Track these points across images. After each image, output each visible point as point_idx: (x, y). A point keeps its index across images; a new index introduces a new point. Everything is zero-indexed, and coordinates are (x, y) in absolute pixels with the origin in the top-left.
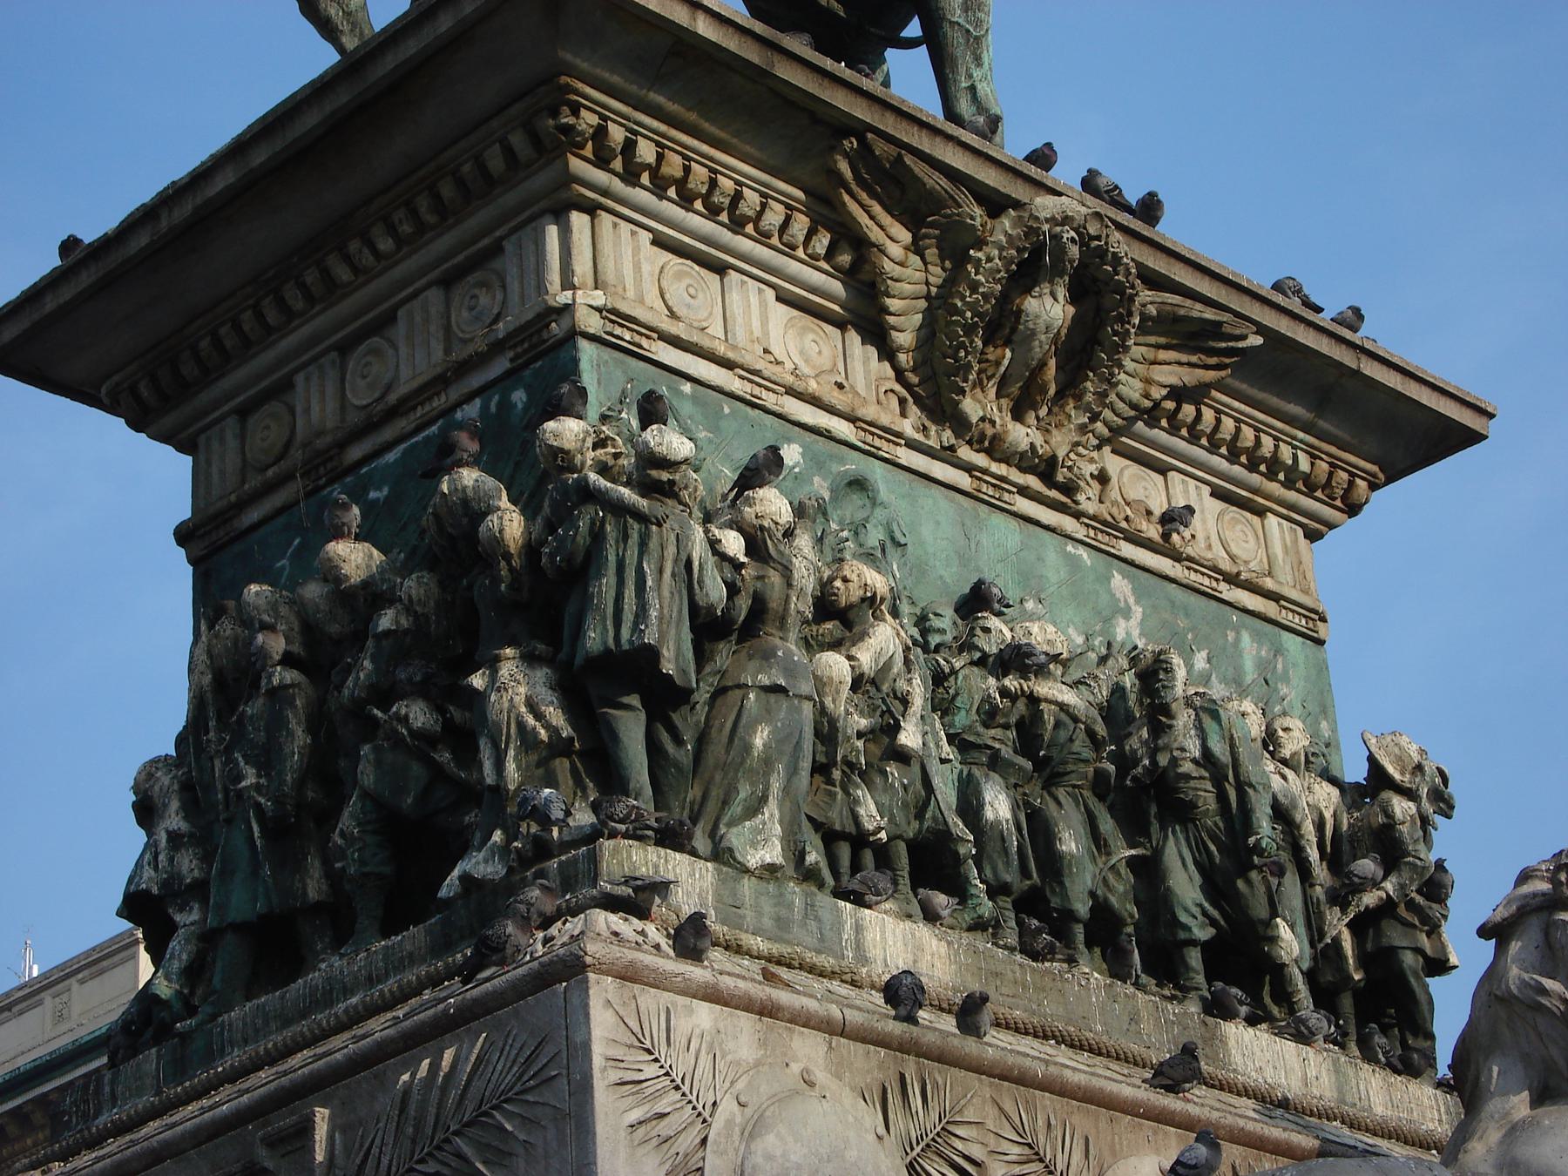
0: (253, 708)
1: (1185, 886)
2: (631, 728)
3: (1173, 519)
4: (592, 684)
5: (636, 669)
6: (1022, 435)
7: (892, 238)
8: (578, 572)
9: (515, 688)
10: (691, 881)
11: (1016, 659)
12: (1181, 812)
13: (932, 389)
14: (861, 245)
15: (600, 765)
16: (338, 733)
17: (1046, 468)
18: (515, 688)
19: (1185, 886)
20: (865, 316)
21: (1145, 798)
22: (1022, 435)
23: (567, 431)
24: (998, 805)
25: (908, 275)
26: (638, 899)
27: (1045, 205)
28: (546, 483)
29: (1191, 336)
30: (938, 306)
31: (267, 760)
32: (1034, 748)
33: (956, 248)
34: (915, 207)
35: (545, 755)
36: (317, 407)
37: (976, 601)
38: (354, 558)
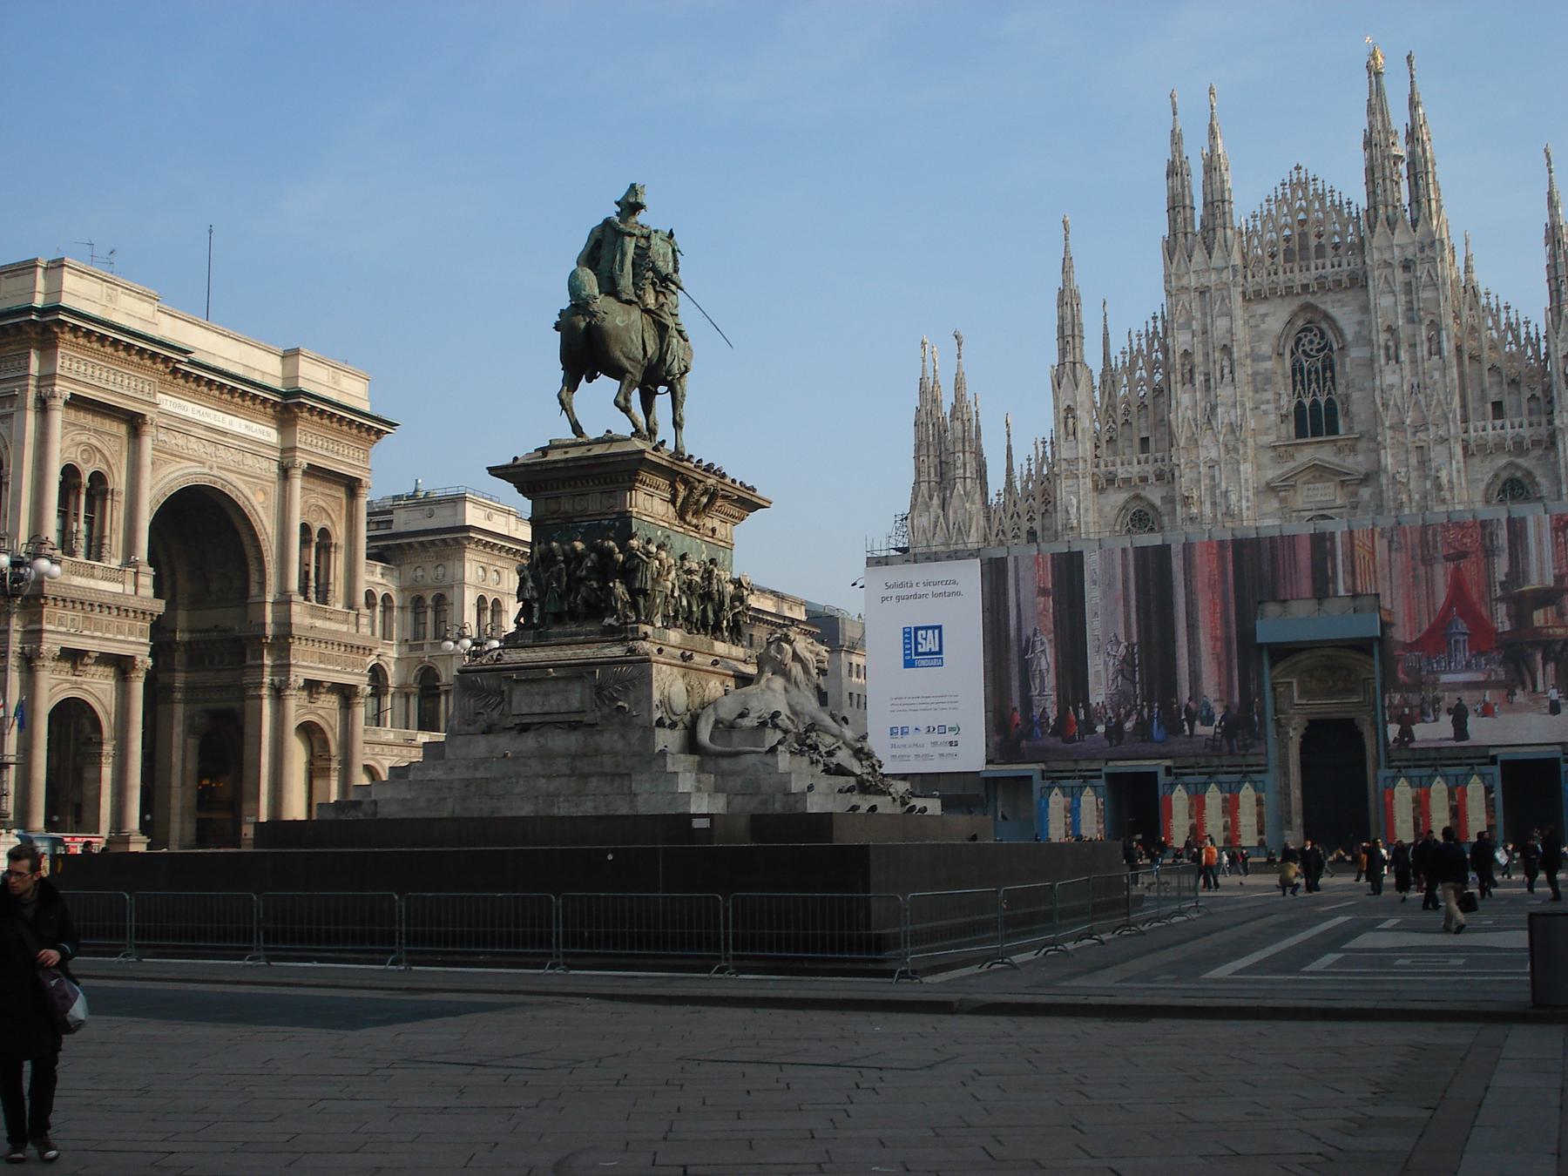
0: (554, 569)
1: (711, 615)
2: (641, 601)
3: (713, 530)
4: (634, 592)
5: (644, 592)
6: (694, 521)
7: (681, 488)
8: (635, 570)
9: (619, 588)
10: (648, 629)
11: (690, 572)
12: (712, 600)
13: (681, 515)
14: (675, 489)
15: (634, 606)
16: (575, 583)
17: (696, 527)
18: (619, 588)
19: (711, 615)
20: (673, 502)
21: (706, 597)
22: (694, 521)
23: (634, 543)
24: (685, 603)
25: (682, 491)
26: (646, 637)
27: (710, 481)
28: (631, 554)
29: (724, 497)
30: (686, 499)
31: (559, 581)
32: (689, 588)
33: (691, 489)
34: (686, 482)
35: (624, 603)
36: (567, 505)
37: (683, 557)
38: (579, 546)
